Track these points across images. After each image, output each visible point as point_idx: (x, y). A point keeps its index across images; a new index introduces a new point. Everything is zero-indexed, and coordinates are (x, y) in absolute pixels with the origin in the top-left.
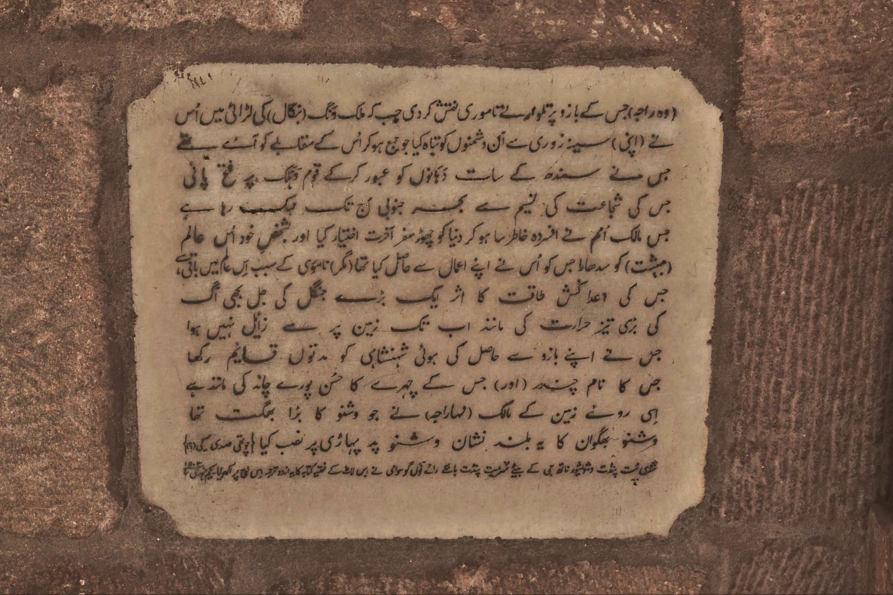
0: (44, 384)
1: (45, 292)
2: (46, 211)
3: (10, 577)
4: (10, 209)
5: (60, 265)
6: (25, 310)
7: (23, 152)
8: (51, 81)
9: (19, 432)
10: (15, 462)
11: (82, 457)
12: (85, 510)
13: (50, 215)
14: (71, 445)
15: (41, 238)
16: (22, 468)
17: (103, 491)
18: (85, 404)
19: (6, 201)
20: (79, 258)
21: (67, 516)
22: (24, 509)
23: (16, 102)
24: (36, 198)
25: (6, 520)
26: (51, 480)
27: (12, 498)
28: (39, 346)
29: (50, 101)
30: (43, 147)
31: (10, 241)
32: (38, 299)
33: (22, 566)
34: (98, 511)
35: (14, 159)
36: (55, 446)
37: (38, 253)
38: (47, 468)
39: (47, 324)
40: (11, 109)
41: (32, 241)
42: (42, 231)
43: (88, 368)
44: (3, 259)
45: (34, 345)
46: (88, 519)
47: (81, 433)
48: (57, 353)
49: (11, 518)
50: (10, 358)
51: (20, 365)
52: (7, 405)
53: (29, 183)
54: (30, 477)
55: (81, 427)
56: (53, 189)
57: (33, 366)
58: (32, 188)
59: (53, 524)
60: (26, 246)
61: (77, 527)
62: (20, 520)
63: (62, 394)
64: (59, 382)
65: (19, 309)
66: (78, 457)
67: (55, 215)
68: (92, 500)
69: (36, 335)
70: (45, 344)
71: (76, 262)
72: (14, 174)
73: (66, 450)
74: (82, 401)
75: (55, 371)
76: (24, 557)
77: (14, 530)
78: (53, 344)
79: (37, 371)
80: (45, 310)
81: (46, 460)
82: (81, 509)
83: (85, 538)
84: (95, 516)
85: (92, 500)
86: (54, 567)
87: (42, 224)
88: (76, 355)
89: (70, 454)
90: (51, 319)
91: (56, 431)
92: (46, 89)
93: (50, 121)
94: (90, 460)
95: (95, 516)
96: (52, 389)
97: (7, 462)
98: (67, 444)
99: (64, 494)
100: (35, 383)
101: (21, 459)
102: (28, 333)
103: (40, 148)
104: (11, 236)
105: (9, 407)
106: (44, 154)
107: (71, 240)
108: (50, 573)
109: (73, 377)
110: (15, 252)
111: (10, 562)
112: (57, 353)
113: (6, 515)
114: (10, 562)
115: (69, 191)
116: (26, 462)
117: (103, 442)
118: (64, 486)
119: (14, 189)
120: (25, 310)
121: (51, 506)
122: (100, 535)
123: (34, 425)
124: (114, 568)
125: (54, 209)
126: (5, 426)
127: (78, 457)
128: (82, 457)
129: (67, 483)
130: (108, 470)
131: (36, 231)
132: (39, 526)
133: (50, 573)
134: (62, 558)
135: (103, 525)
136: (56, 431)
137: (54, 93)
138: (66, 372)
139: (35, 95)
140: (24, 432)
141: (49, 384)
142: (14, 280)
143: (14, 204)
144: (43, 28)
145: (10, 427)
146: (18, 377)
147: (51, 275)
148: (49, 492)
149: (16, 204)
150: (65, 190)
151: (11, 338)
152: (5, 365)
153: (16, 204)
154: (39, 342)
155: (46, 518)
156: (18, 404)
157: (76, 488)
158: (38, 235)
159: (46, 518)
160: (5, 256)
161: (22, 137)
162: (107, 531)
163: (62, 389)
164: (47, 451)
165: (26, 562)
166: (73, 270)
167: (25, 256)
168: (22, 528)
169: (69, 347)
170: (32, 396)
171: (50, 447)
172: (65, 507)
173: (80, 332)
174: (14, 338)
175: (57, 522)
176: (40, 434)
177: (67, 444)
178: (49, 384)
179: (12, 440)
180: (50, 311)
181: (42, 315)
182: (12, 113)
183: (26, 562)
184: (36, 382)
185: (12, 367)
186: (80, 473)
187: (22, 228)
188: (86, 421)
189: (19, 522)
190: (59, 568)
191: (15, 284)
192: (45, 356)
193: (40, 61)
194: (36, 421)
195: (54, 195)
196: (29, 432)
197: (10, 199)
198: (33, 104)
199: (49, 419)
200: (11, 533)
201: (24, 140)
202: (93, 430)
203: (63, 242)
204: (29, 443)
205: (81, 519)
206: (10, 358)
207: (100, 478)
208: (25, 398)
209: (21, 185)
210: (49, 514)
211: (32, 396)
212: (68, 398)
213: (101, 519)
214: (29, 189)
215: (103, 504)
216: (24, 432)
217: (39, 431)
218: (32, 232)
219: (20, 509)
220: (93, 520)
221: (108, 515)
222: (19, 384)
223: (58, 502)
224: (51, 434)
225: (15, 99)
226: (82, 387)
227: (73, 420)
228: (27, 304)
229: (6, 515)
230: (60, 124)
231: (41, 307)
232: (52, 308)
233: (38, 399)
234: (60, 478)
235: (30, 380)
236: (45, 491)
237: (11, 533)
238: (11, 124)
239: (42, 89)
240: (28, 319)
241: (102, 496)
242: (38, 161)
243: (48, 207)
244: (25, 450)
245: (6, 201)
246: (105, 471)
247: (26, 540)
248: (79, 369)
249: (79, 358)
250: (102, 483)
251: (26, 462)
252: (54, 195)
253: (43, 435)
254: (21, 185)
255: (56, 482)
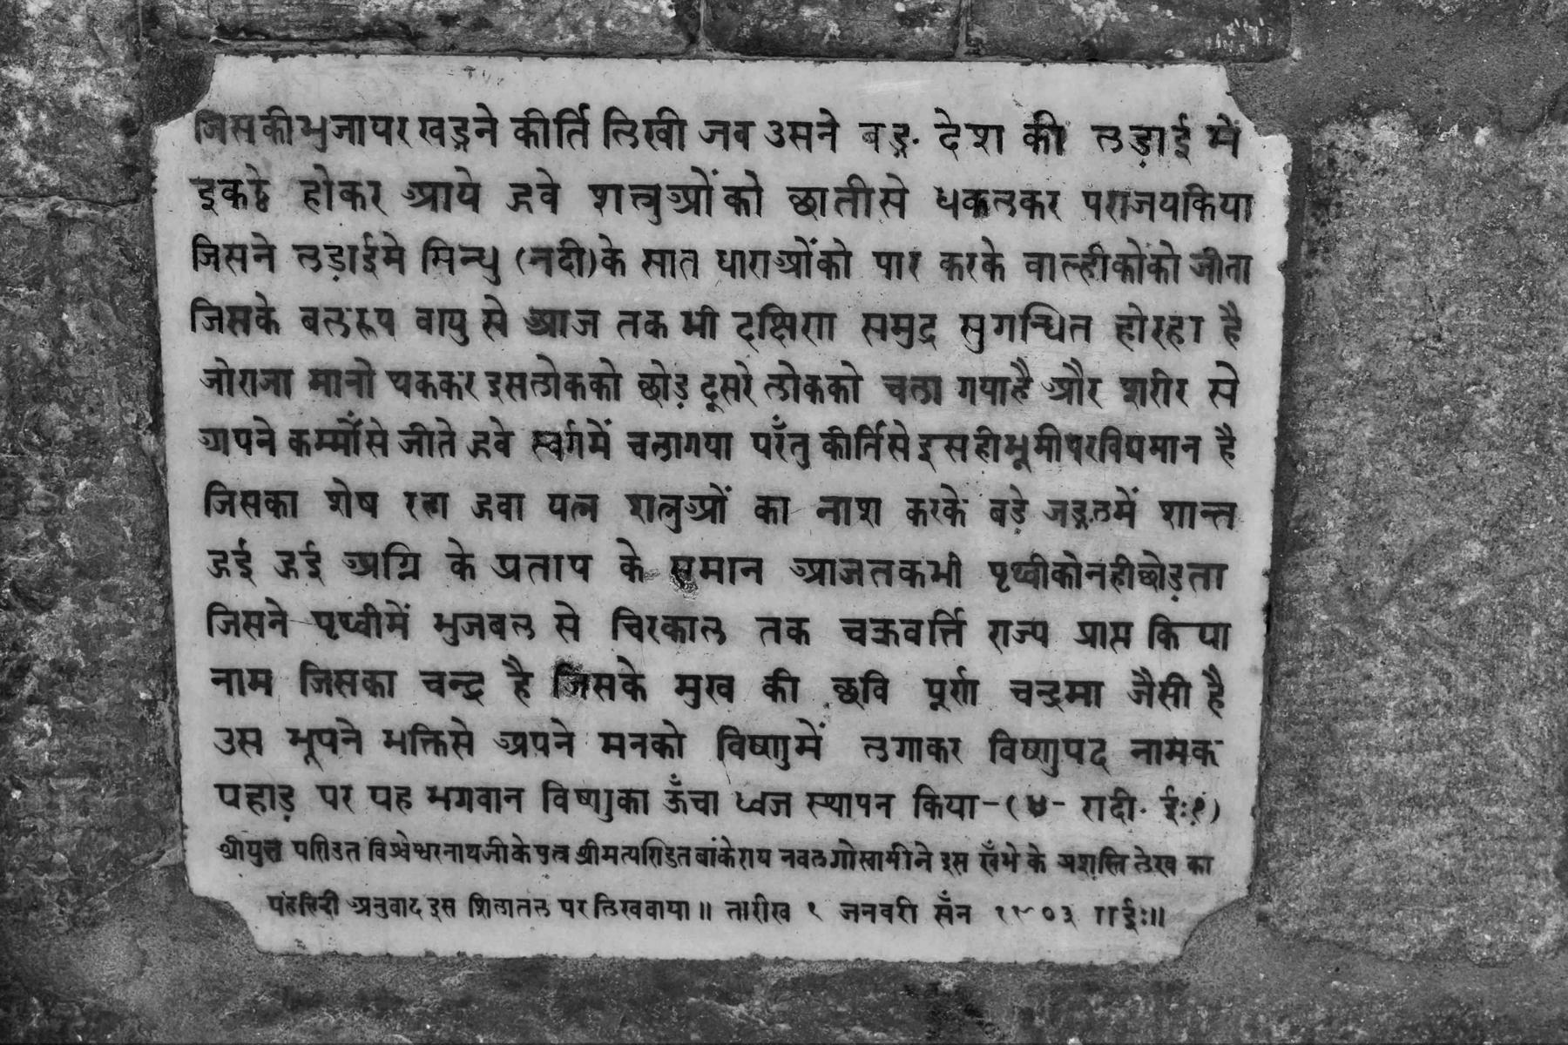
0: (1461, 680)
1: (1488, 508)
2: (1509, 358)
3: (1354, 1032)
4: (1443, 354)
5: (1521, 460)
6: (1444, 542)
7: (1482, 246)
8: (1550, 115)
9: (1408, 768)
10: (1393, 823)
11: (1517, 816)
12: (1511, 914)
13: (1516, 367)
14: (1499, 793)
15: (1493, 408)
16: (1403, 833)
17: (1547, 880)
18: (1535, 718)
19: (1439, 338)
20: (1558, 447)
21: (1475, 925)
22: (1397, 909)
23: (1478, 155)
24: (1495, 333)
25: (1361, 928)
26: (1454, 856)
27: (1377, 889)
28: (1461, 609)
29: (1542, 152)
30: (1518, 237)
31: (1435, 414)
32: (1471, 522)
33: (1381, 1013)
34: (1533, 917)
35: (1465, 260)
36: (1468, 795)
37: (1485, 437)
38: (1449, 835)
39: (1481, 568)
40: (1467, 166)
41: (1477, 413)
42: (1497, 396)
43: (1550, 651)
44: (1419, 446)
45: (1453, 607)
46: (1512, 932)
47: (1519, 772)
48: (1495, 622)
49: (1369, 926)
50: (1405, 630)
51: (1423, 644)
52: (1390, 716)
53: (1485, 307)
54: (1415, 851)
55: (1521, 761)
56: (1530, 318)
57: (1445, 645)
58: (1490, 314)
59: (1448, 939)
60: (1465, 423)
61: (1490, 945)
62: (1385, 930)
63: (1491, 702)
64: (1492, 678)
65: (1434, 540)
66: (1509, 816)
67: (1527, 366)
68: (1524, 896)
69: (1460, 589)
70: (1473, 607)
71: (1553, 454)
72: (1460, 289)
73: (1489, 802)
74: (1532, 714)
75: (1487, 656)
76: (1387, 997)
77: (1374, 948)
78: (1490, 606)
79: (1453, 655)
80: (1484, 543)
81: (1450, 820)
82: (1503, 912)
83: (1504, 964)
84: (1526, 925)
85: (1524, 896)
86: (1438, 1018)
87: (1500, 382)
88: (1529, 628)
89: (1495, 810)
90: (1490, 559)
91: (1474, 767)
92: (1539, 131)
93: (1538, 189)
94: (1530, 822)
95: (1526, 925)
96: (1476, 690)
97: (1379, 822)
98: (1493, 791)
99: (1475, 883)
100: (1445, 677)
101: (1404, 818)
102: (1445, 584)
103: (1513, 241)
104: (1437, 404)
105: (1394, 720)
106: (1519, 252)
107: (1550, 414)
108: (1430, 1026)
109: (1519, 667)
110: (1443, 432)
111: (1360, 1006)
112: (1495, 622)
113: (1361, 921)
114: (1360, 1006)
115: (1557, 321)
116: (1412, 822)
117: (1559, 789)
118: (1475, 868)
119: (1456, 315)
120: (1444, 542)
121: (1449, 904)
122: (1531, 960)
123: (1436, 755)
124: (1549, 1023)
125: (1525, 355)
126: (1383, 756)
127: (1509, 816)
128: (1517, 816)
129: (1482, 863)
130: (1561, 841)
131: (1486, 394)
132: (1422, 941)
133: (1430, 1026)
134: (1456, 1002)
135: (1538, 943)
136: (1474, 767)
137: (1551, 135)
138: (1507, 658)
139: (1513, 141)
140: (1416, 767)
141: (1473, 678)
142: (1432, 485)
143: (1453, 344)
144: (1551, 15)
145: (1391, 757)
146: (1417, 666)
147: (1502, 478)
148: (1448, 877)
149: (1455, 345)
150: (1549, 319)
151: (1412, 594)
152: (1397, 642)
153: (1455, 345)
154: (1462, 601)
155: (1436, 927)
156: (1411, 715)
157: (1500, 872)
158: (1489, 402)
159: (1436, 927)
160: (1422, 440)
161: (1481, 218)
162: (1546, 953)
163: (1495, 689)
164: (1453, 804)
165: (1389, 1005)
166: (1546, 468)
167: (1459, 440)
168: (1392, 944)
169: (1518, 614)
170: (1437, 701)
171: (1459, 797)
172: (1473, 908)
173: (1542, 584)
174: (1417, 594)
175: (1457, 933)
176: (1444, 772)
177: (1493, 791)
178: (1473, 678)
179: (1392, 781)
180: (1491, 545)
181: (1475, 550)
182: (1470, 175)
183: (1389, 1005)
184: (1449, 675)
185: (1407, 647)
186: (1508, 846)
187: (1462, 389)
188: (1533, 749)
189: (1385, 933)
190: (1450, 1018)
191: (1432, 493)
192: (1472, 627)
193: (1534, 77)
194: (1440, 748)
195: (1528, 328)
196: (1425, 767)
197: (1445, 335)
198: (1508, 159)
199: (1464, 744)
200: (1368, 953)
201: (1484, 225)
202: (1544, 766)
203: (1534, 415)
204: (1423, 787)
205: (1499, 931)
206: (1405, 630)
207: (1544, 855)
208: (1425, 705)
209: (1469, 309)
210: (1440, 919)
211: (1437, 701)
212: (1504, 705)
213: (1537, 932)
214: (1483, 316)
215: (1546, 904)
216: (1416, 767)
217: (1445, 765)
218: (1478, 397)
219: (1390, 908)
220: (1521, 933)
221: (1550, 924)
222: (1416, 678)
223: (1462, 899)
224: (1467, 771)
225: (1477, 149)
226: (1534, 688)
227: (1507, 747)
228: (1450, 532)
229: (1361, 921)
230: (1557, 196)
231: (1475, 537)
232: (1495, 540)
233: (1448, 706)
234: (1469, 854)
235: (1437, 672)
236: (1440, 877)
237: (1368, 953)
238: (1464, 194)
239: (1528, 131)
240: (1448, 558)
241: (1545, 889)
242: (1508, 266)
243: (1516, 350)
244: (1416, 802)
245: (1439, 338)
246: (1554, 843)
247: (1395, 966)
248: (1531, 652)
249: (1535, 631)
250: (1546, 865)
251: (1412, 822)
252: (1528, 328)
253: (1450, 774)
254: (1469, 309)
255: (1463, 860)
